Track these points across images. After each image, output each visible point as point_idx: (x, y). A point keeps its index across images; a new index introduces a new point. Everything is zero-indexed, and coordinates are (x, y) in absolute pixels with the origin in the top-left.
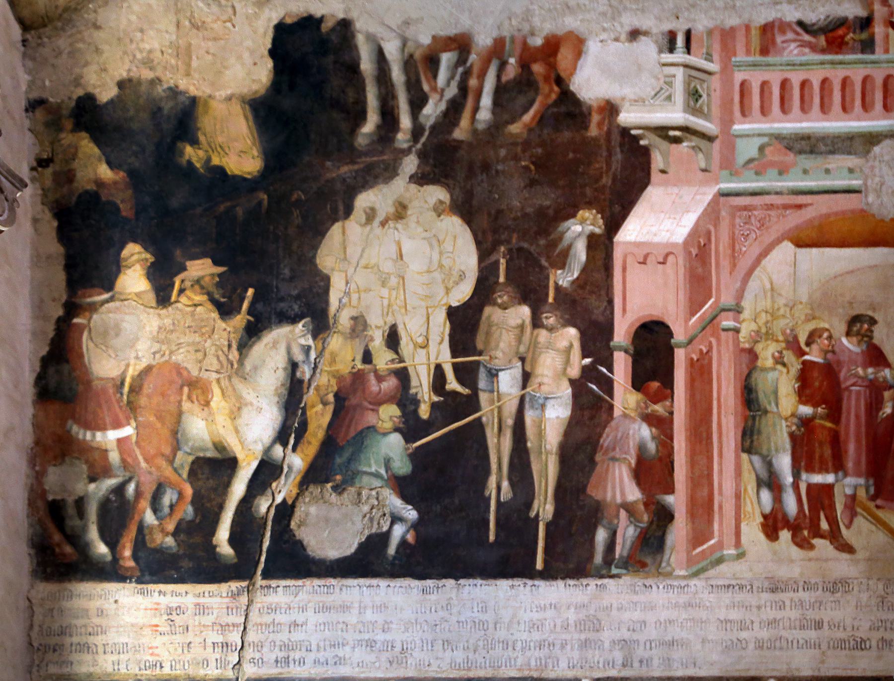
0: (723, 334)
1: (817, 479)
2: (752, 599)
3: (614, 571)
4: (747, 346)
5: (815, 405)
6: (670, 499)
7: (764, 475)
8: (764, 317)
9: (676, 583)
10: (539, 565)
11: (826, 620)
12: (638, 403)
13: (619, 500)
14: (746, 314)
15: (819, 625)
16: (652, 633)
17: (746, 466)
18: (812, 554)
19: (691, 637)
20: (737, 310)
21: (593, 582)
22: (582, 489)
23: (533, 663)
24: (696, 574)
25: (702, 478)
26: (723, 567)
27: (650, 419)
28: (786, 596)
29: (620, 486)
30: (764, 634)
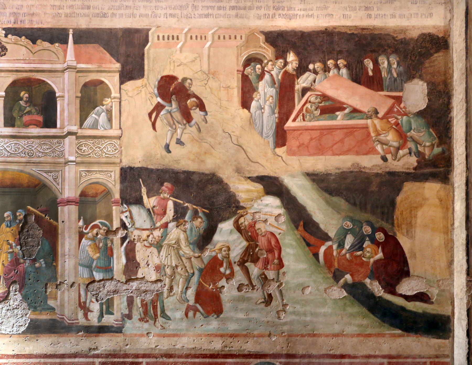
11: (91, 5)
15: (89, 8)
16: (25, 10)
19: (40, 12)
30: (68, 11)
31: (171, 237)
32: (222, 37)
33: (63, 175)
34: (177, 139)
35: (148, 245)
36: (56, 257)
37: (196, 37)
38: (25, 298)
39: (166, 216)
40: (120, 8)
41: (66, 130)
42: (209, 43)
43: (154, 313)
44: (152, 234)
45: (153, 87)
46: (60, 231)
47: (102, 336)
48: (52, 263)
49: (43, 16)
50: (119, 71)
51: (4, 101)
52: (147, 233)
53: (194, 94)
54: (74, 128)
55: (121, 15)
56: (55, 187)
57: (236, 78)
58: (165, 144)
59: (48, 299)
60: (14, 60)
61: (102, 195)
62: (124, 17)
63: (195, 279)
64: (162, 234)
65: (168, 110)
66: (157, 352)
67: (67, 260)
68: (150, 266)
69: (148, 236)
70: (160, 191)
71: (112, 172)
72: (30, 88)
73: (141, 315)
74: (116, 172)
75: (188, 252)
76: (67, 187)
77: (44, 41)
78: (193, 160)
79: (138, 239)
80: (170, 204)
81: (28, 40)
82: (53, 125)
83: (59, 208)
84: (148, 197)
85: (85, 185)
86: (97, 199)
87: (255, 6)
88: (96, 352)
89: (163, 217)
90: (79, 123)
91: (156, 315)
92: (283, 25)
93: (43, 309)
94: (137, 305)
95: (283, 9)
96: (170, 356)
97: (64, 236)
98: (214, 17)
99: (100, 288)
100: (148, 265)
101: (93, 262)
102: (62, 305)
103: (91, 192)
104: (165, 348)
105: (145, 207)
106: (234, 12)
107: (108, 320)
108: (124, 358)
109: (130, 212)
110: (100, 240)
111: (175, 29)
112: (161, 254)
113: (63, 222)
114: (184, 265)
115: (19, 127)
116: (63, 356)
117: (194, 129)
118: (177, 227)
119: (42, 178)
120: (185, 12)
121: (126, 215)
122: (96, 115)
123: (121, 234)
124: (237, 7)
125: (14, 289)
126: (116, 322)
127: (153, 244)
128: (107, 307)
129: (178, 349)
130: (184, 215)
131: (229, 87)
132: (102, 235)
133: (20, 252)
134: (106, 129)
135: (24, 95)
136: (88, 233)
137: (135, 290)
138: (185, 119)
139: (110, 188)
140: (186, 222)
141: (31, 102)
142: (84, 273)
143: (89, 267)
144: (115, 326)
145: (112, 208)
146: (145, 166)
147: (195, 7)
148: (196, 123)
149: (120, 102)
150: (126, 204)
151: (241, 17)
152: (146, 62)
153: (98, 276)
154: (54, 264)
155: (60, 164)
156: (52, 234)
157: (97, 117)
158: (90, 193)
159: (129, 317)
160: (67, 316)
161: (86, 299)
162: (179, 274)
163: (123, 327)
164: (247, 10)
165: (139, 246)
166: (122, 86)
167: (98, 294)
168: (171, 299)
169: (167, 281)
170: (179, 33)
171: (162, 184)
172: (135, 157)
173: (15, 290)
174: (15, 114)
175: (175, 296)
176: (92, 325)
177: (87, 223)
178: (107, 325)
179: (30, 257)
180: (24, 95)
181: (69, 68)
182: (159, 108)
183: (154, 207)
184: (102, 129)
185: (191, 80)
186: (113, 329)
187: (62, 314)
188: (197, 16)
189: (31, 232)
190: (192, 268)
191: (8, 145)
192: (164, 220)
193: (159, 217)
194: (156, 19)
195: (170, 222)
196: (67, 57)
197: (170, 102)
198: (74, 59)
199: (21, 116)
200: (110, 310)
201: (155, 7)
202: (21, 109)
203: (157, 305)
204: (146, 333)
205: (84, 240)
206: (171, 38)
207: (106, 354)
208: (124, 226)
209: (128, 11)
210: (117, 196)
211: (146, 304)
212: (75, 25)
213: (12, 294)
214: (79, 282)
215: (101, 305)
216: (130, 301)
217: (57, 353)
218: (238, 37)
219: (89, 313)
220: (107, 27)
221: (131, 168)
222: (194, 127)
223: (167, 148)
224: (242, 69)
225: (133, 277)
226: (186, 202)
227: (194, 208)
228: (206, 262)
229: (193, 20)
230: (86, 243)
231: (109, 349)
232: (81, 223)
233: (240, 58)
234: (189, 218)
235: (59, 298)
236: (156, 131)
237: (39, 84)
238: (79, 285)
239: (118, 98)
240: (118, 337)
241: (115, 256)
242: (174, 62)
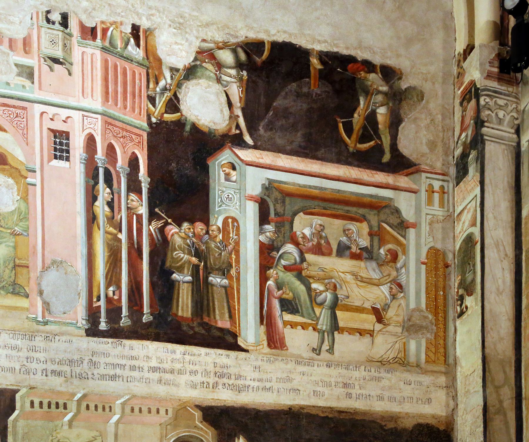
32: (137, 410)
37: (96, 407)
87: (188, 370)
92: (229, 399)
95: (229, 378)
98: (125, 380)
106: (156, 376)
111: (59, 393)
120: (78, 370)
124: (160, 369)
151: (167, 383)
164: (176, 374)
170: (68, 400)
188: (97, 376)
194: (28, 377)
201: (27, 358)
206: (53, 406)
218: (162, 412)
229: (91, 382)
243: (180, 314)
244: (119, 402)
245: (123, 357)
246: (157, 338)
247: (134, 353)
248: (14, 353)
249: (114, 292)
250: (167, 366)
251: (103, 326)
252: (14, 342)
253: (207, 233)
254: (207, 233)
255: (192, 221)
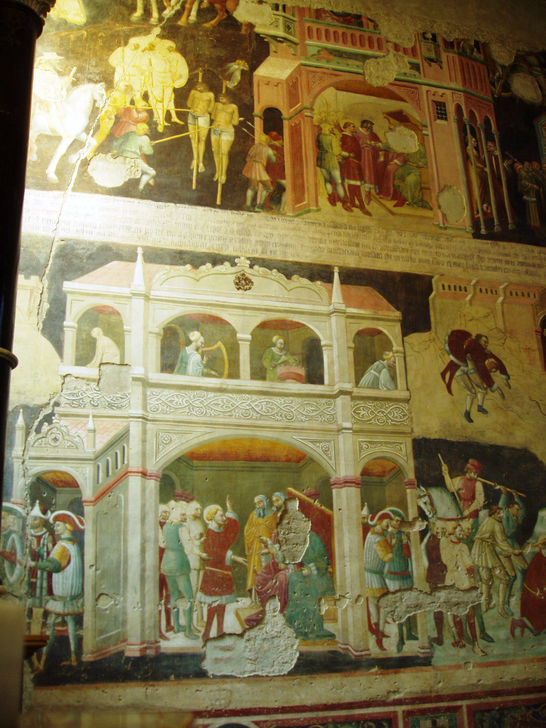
0: (306, 118)
1: (353, 182)
2: (326, 230)
3: (257, 209)
4: (317, 124)
5: (350, 152)
6: (283, 182)
7: (328, 177)
8: (323, 115)
9: (287, 218)
10: (218, 202)
11: (361, 243)
12: (266, 140)
13: (258, 179)
14: (316, 112)
15: (357, 245)
17: (319, 173)
18: (352, 214)
20: (312, 110)
21: (246, 214)
22: (240, 172)
23: (215, 247)
24: (297, 216)
25: (298, 176)
26: (310, 214)
27: (272, 147)
28: (342, 231)
29: (258, 173)
30: (332, 246)
31: (484, 529)
32: (514, 294)
33: (336, 446)
34: (479, 406)
35: (455, 540)
36: (332, 560)
37: (486, 290)
38: (290, 621)
39: (476, 501)
40: (394, 250)
41: (337, 388)
42: (501, 299)
43: (471, 633)
44: (460, 525)
45: (443, 342)
46: (336, 523)
47: (403, 672)
48: (327, 569)
49: (300, 248)
50: (400, 321)
51: (250, 345)
52: (452, 524)
53: (491, 353)
54: (348, 386)
55: (397, 258)
56: (327, 463)
57: (535, 339)
58: (464, 411)
59: (324, 621)
60: (263, 296)
61: (391, 474)
62: (401, 260)
63: (518, 584)
64: (472, 525)
65: (463, 371)
66: (480, 689)
67: (348, 564)
68: (460, 569)
69: (455, 528)
70: (465, 470)
71: (401, 443)
72: (286, 332)
73: (454, 638)
74: (407, 444)
75: (505, 548)
76: (342, 462)
77: (303, 277)
78: (500, 432)
79: (442, 532)
80: (479, 487)
81: (280, 274)
82: (320, 381)
83: (334, 491)
84: (451, 478)
85: (367, 460)
86: (385, 479)
88: (397, 696)
89: (472, 503)
90: (354, 381)
91: (474, 636)
93: (318, 636)
94: (448, 622)
96: (495, 693)
97: (342, 530)
99: (396, 602)
100: (458, 568)
101: (384, 566)
102: (345, 630)
103: (377, 469)
104: (490, 683)
105: (448, 491)
106: (523, 268)
107: (411, 648)
108: (436, 702)
109: (430, 497)
110: (392, 534)
112: (473, 551)
113: (340, 509)
114: (503, 566)
115: (272, 380)
116: (350, 706)
117: (496, 394)
118: (490, 515)
119: (309, 450)
120: (471, 262)
121: (425, 501)
122: (375, 370)
123: (419, 526)
125: (272, 607)
126: (422, 651)
127: (462, 539)
128: (409, 629)
129: (507, 683)
130: (496, 500)
131: (529, 348)
132: (394, 528)
133: (280, 553)
134: (389, 390)
135: (278, 340)
136: (375, 526)
137: (445, 602)
138: (485, 382)
139: (401, 465)
140: (500, 509)
141: (288, 350)
142: (374, 582)
143: (379, 573)
144: (421, 656)
145: (405, 491)
146: (444, 438)
147: (481, 259)
148: (498, 387)
149: (405, 358)
150: (423, 486)
151: (532, 274)
152: (432, 313)
153: (392, 585)
154: (330, 570)
155: (331, 431)
156: (324, 526)
157: (377, 374)
158: (374, 471)
159: (439, 641)
160: (352, 645)
161: (379, 619)
162: (497, 577)
163: (432, 657)
165: (444, 542)
166: (406, 339)
167: (394, 611)
168: (492, 612)
169: (484, 588)
171: (467, 462)
172: (431, 426)
173: (274, 609)
174: (266, 363)
175: (497, 607)
176: (389, 656)
177: (373, 511)
178: (410, 655)
179: (293, 560)
180: (278, 340)
181: (336, 311)
182: (452, 368)
183: (459, 490)
184: (385, 389)
185: (486, 337)
186: (419, 661)
187: (346, 642)
188: (484, 268)
189: (293, 525)
190: (513, 569)
191: (256, 403)
192: (474, 506)
193: (466, 502)
195: (480, 510)
196: (333, 298)
197: (465, 362)
198: (342, 302)
199: (275, 367)
200: (413, 633)
202: (273, 357)
203: (474, 622)
204: (463, 662)
205: (369, 535)
206: (458, 289)
207: (412, 699)
208: (422, 515)
209: (404, 254)
210: (411, 475)
211: (460, 621)
212: (341, 264)
213: (268, 616)
214: (367, 595)
215: (400, 626)
216: (439, 618)
217: (343, 701)
218: (532, 296)
219: (384, 640)
220: (382, 269)
221: (425, 440)
222: (496, 392)
223: (468, 415)
224: (540, 329)
225: (439, 585)
226: (499, 484)
227: (508, 492)
228: (529, 561)
229: (480, 272)
230: (373, 540)
231: (415, 690)
232: (365, 512)
233: (536, 318)
234: (504, 505)
235: (340, 620)
236: (452, 395)
237: (298, 327)
238: (367, 599)
239: (401, 353)
240: (426, 671)
241: (413, 556)
242: (464, 315)
243: (532, 224)
244: (501, 287)
245: (500, 254)
246: (519, 241)
247: (506, 252)
248: (427, 249)
249: (487, 207)
250: (530, 261)
251: (483, 231)
252: (426, 241)
253: (541, 169)
254: (541, 169)
255: (530, 161)
